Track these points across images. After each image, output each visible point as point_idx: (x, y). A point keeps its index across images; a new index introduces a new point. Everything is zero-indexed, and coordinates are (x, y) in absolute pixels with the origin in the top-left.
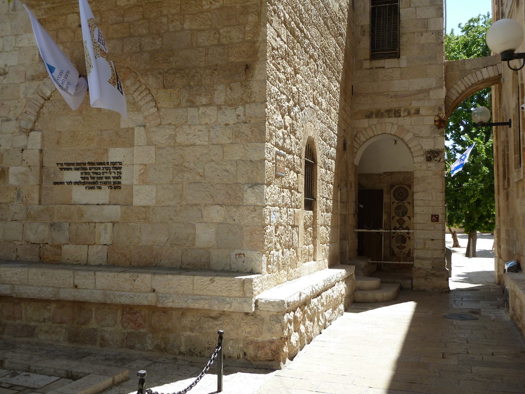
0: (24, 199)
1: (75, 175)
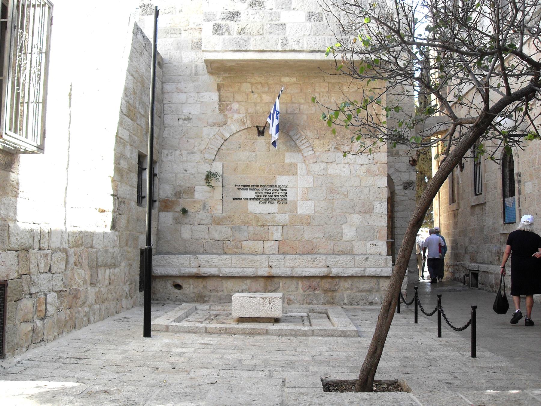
0: (209, 210)
1: (251, 194)
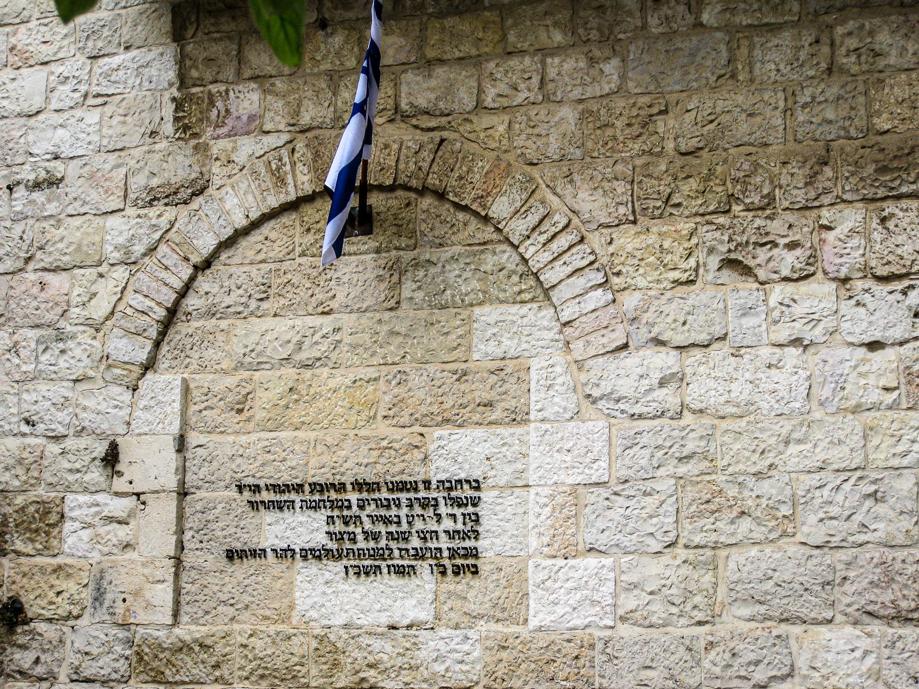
0: (120, 608)
1: (307, 528)
